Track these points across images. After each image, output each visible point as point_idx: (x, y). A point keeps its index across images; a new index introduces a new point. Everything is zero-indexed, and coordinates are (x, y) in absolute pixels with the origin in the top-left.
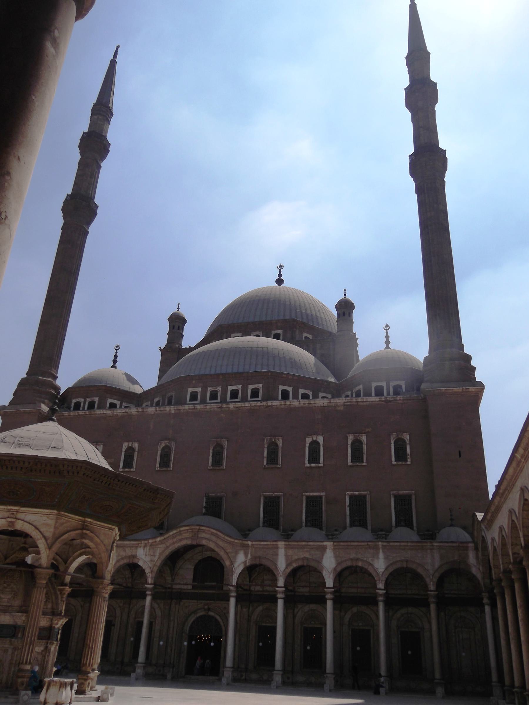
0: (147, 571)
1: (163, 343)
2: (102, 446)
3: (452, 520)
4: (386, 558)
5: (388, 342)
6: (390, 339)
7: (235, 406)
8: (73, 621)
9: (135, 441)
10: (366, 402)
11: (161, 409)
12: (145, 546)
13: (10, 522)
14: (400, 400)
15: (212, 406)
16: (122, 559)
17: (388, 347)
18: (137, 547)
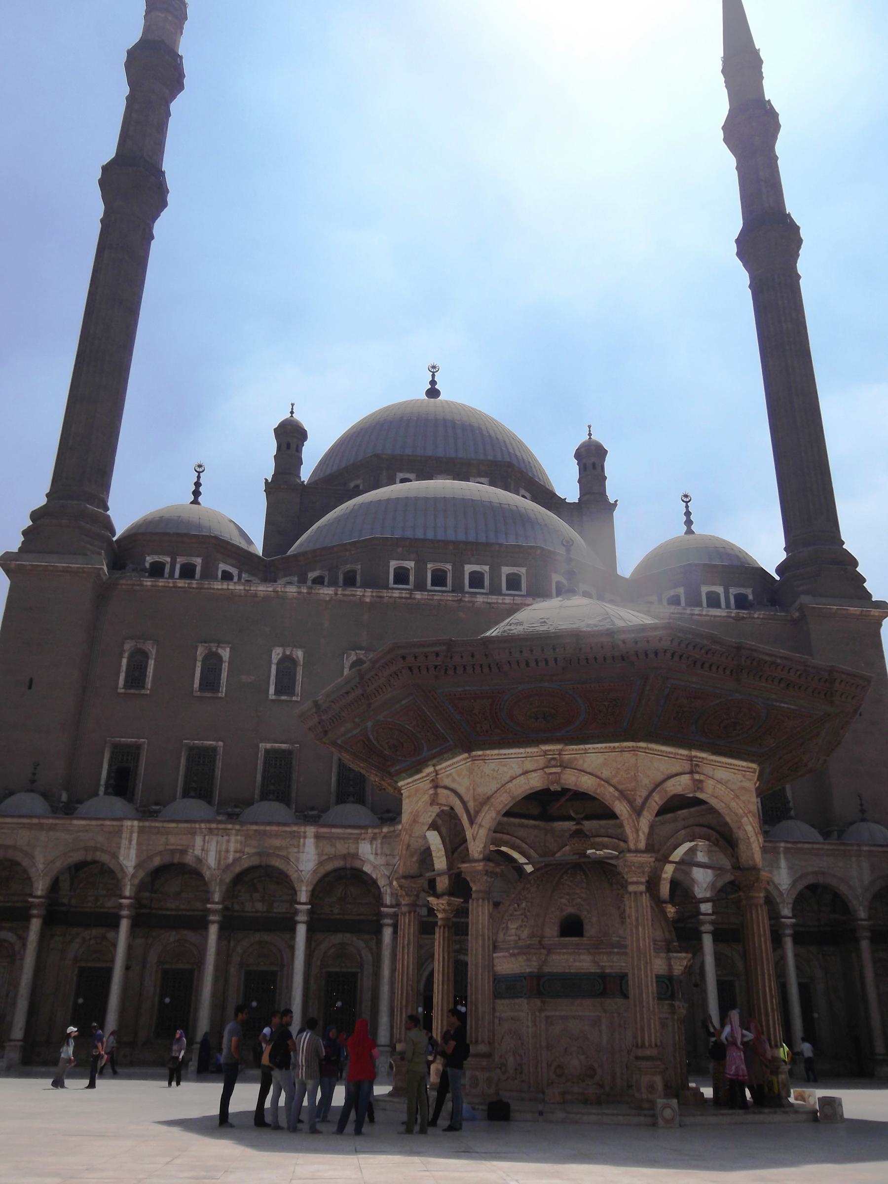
0: (381, 882)
1: (268, 470)
2: (228, 650)
3: (863, 811)
4: (791, 868)
5: (689, 523)
6: (692, 517)
7: (486, 600)
8: (196, 973)
9: (301, 647)
10: (706, 615)
11: (347, 593)
12: (373, 839)
13: (701, 781)
14: (758, 618)
15: (444, 596)
16: (330, 859)
17: (689, 532)
18: (357, 839)
